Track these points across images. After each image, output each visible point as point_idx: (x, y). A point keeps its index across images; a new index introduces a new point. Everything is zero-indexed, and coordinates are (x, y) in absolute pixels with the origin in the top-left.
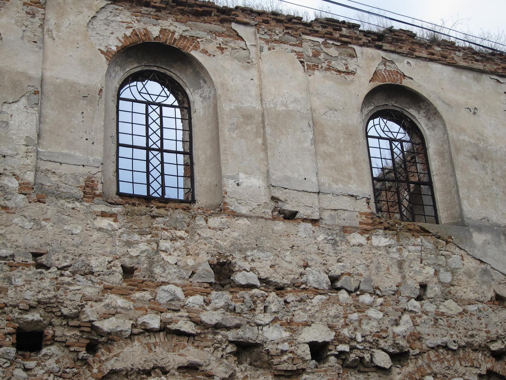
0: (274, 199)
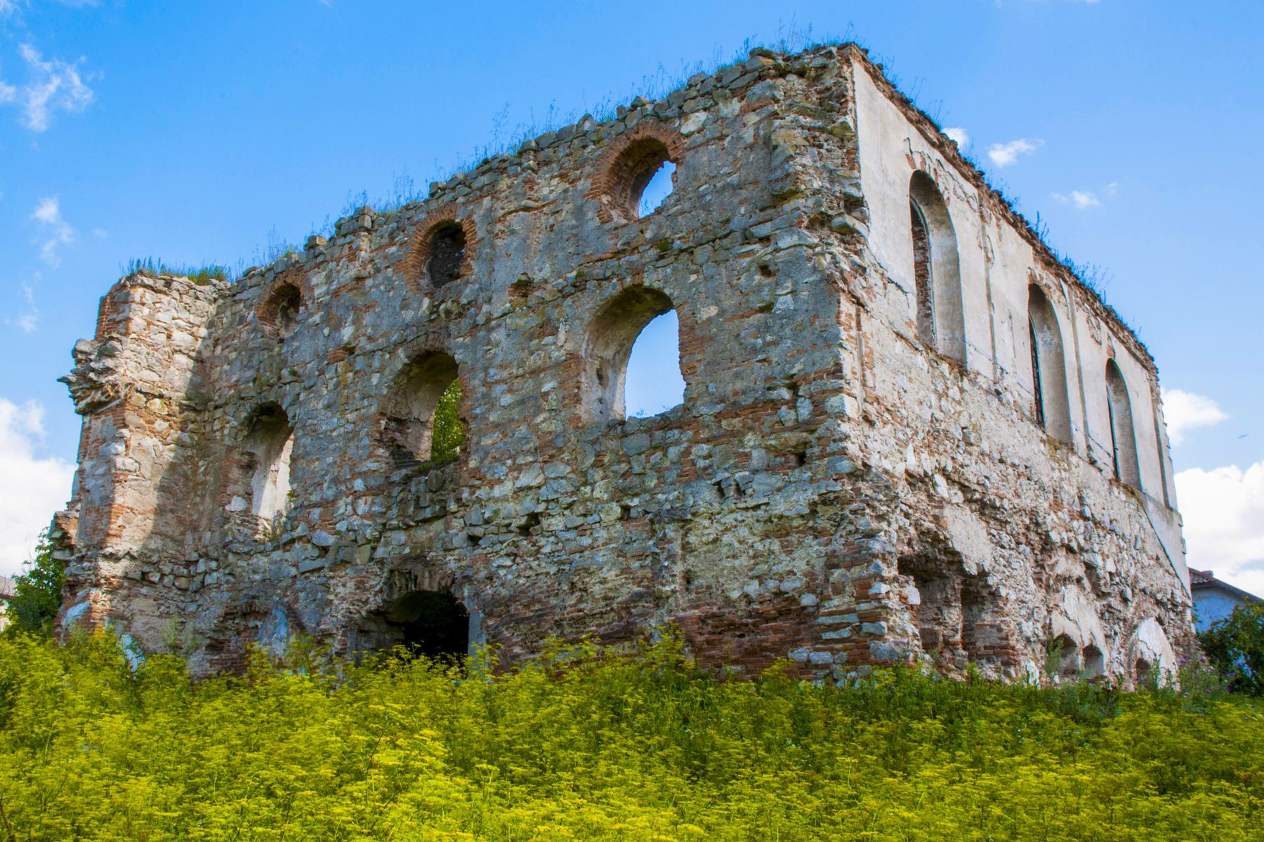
0: (1089, 447)
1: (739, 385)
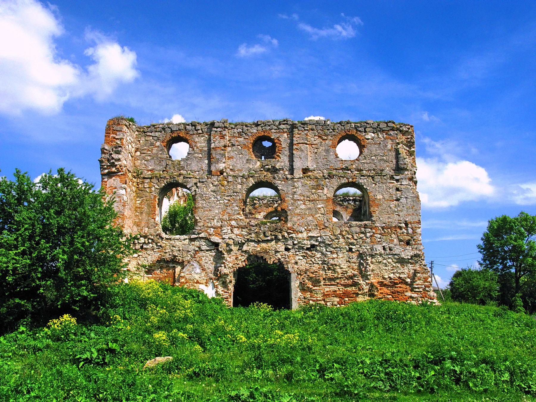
1: (390, 220)
